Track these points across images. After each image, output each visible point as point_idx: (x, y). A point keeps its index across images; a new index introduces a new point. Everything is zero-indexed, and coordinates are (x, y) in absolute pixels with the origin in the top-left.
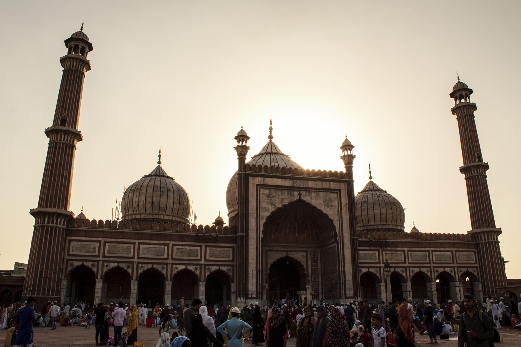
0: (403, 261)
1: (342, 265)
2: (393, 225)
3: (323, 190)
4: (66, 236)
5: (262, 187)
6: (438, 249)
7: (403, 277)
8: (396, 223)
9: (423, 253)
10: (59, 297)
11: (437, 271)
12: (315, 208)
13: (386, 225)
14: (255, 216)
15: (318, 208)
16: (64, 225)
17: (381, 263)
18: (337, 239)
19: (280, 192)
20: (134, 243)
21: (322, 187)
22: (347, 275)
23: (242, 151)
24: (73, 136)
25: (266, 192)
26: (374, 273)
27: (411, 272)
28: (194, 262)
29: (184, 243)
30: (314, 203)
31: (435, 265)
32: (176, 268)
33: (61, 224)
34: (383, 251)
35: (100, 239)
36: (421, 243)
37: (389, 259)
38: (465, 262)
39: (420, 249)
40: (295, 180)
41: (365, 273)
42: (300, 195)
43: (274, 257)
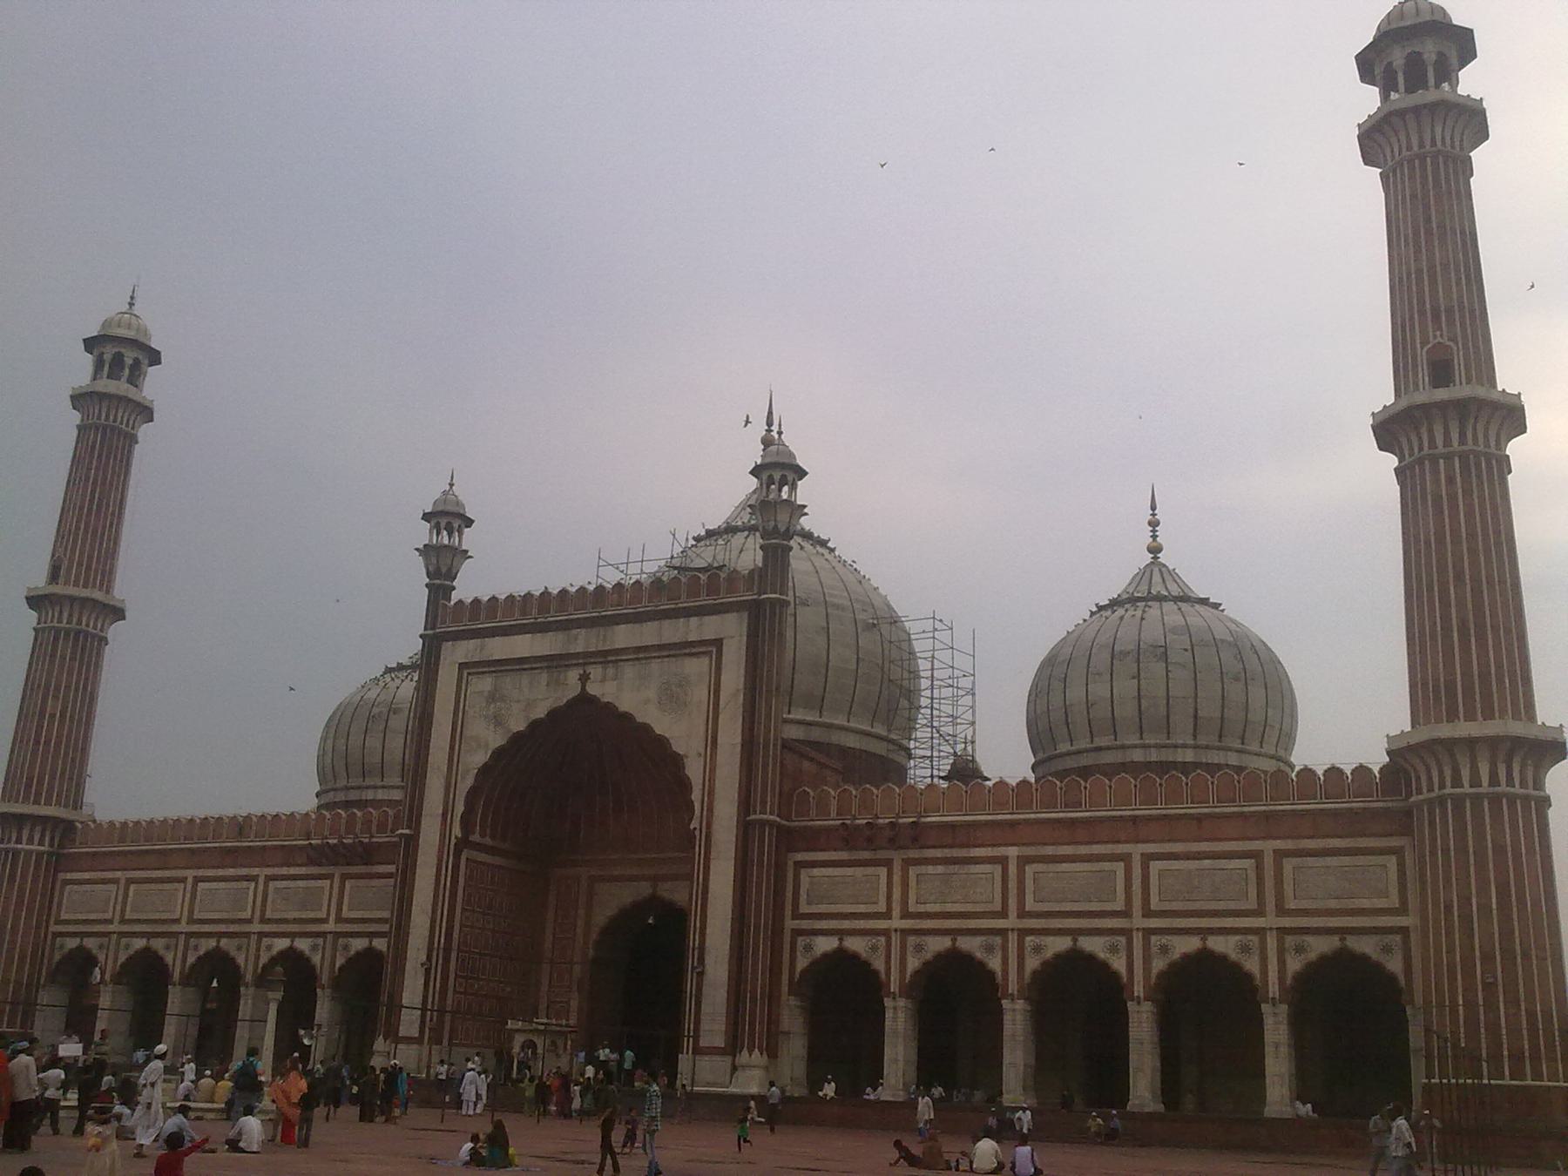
0: (998, 907)
1: (698, 925)
2: (1144, 746)
4: (56, 871)
6: (1178, 848)
7: (992, 974)
10: (17, 1030)
11: (1164, 949)
12: (627, 717)
13: (1109, 748)
15: (638, 720)
17: (896, 912)
18: (692, 827)
19: (525, 679)
20: (183, 880)
22: (709, 960)
24: (76, 607)
25: (484, 684)
26: (864, 955)
29: (293, 871)
30: (624, 705)
31: (1155, 923)
32: (269, 948)
33: (32, 845)
34: (908, 863)
35: (118, 874)
37: (932, 898)
39: (1083, 850)
40: (575, 632)
41: (825, 956)
42: (584, 678)
43: (614, 899)
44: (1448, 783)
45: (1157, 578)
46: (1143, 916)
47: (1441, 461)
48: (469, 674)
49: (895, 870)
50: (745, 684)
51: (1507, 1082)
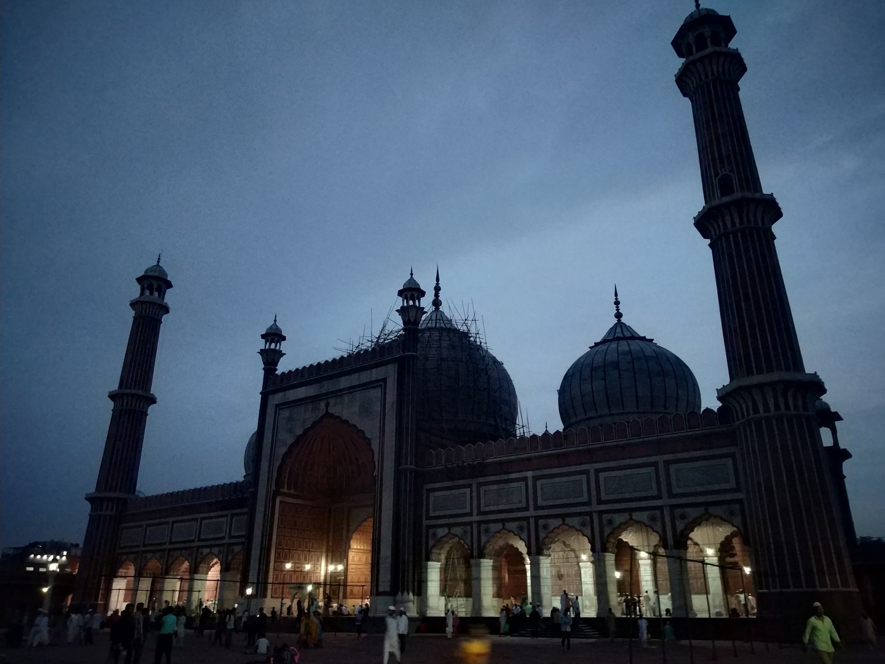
3: (359, 387)
5: (282, 407)
8: (638, 409)
9: (572, 478)
14: (269, 458)
16: (112, 510)
17: (475, 512)
20: (167, 523)
21: (355, 383)
23: (271, 358)
27: (540, 528)
28: (217, 542)
31: (603, 507)
34: (479, 485)
36: (564, 454)
38: (699, 489)
39: (565, 470)
42: (327, 405)
44: (751, 412)
45: (619, 330)
46: (598, 504)
47: (731, 236)
48: (280, 409)
49: (473, 490)
50: (397, 398)
51: (805, 589)
